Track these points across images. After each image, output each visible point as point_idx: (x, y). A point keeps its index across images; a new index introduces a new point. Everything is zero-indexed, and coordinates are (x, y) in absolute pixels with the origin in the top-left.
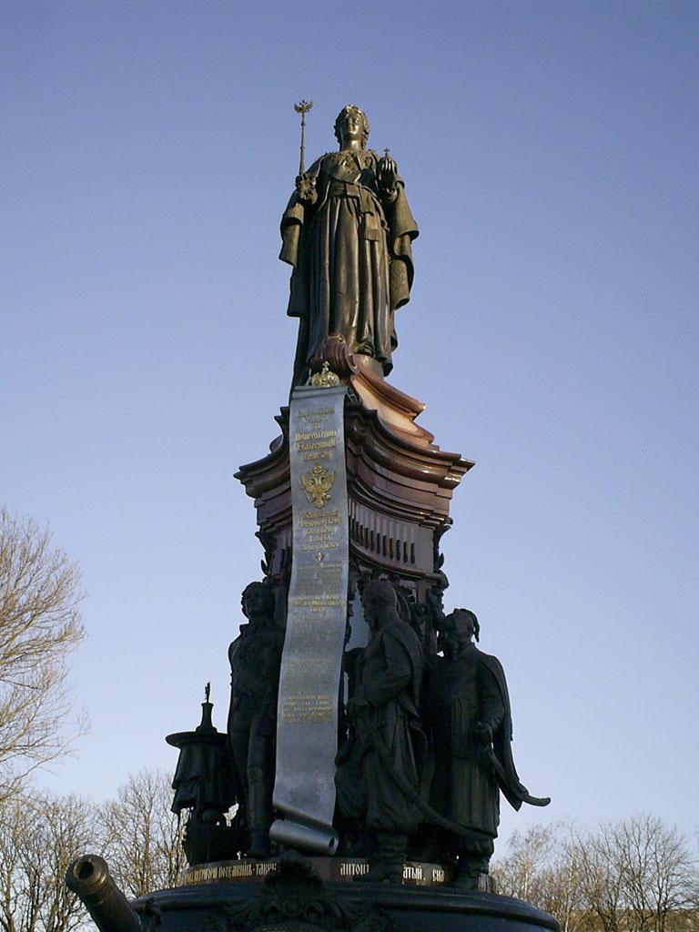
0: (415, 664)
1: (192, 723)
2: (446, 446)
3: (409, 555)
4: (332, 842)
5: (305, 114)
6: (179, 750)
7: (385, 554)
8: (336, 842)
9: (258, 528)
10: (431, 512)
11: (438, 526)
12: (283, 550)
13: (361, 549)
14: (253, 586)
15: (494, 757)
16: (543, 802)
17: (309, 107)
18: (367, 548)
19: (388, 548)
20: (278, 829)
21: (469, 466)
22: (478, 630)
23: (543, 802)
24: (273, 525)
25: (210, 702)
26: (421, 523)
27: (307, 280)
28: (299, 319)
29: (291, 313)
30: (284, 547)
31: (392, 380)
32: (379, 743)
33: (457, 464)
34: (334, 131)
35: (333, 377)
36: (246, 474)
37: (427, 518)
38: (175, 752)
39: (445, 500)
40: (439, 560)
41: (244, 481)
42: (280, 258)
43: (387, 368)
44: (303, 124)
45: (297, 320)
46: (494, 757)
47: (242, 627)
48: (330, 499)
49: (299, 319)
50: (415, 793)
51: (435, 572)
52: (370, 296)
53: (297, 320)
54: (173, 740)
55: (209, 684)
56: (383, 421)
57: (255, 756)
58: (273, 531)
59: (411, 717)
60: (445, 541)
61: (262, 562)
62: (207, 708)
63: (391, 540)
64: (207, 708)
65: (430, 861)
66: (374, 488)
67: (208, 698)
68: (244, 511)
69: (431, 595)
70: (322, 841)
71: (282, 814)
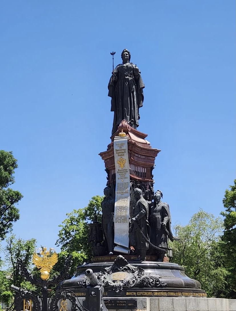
0: (147, 210)
4: (129, 252)
12: (112, 175)
13: (133, 176)
14: (105, 188)
17: (115, 53)
20: (116, 249)
21: (158, 152)
22: (162, 195)
28: (114, 112)
29: (112, 111)
31: (138, 129)
34: (122, 59)
42: (109, 95)
44: (113, 59)
49: (114, 112)
52: (133, 106)
58: (110, 169)
61: (107, 177)
63: (140, 172)
68: (101, 164)
71: (116, 245)
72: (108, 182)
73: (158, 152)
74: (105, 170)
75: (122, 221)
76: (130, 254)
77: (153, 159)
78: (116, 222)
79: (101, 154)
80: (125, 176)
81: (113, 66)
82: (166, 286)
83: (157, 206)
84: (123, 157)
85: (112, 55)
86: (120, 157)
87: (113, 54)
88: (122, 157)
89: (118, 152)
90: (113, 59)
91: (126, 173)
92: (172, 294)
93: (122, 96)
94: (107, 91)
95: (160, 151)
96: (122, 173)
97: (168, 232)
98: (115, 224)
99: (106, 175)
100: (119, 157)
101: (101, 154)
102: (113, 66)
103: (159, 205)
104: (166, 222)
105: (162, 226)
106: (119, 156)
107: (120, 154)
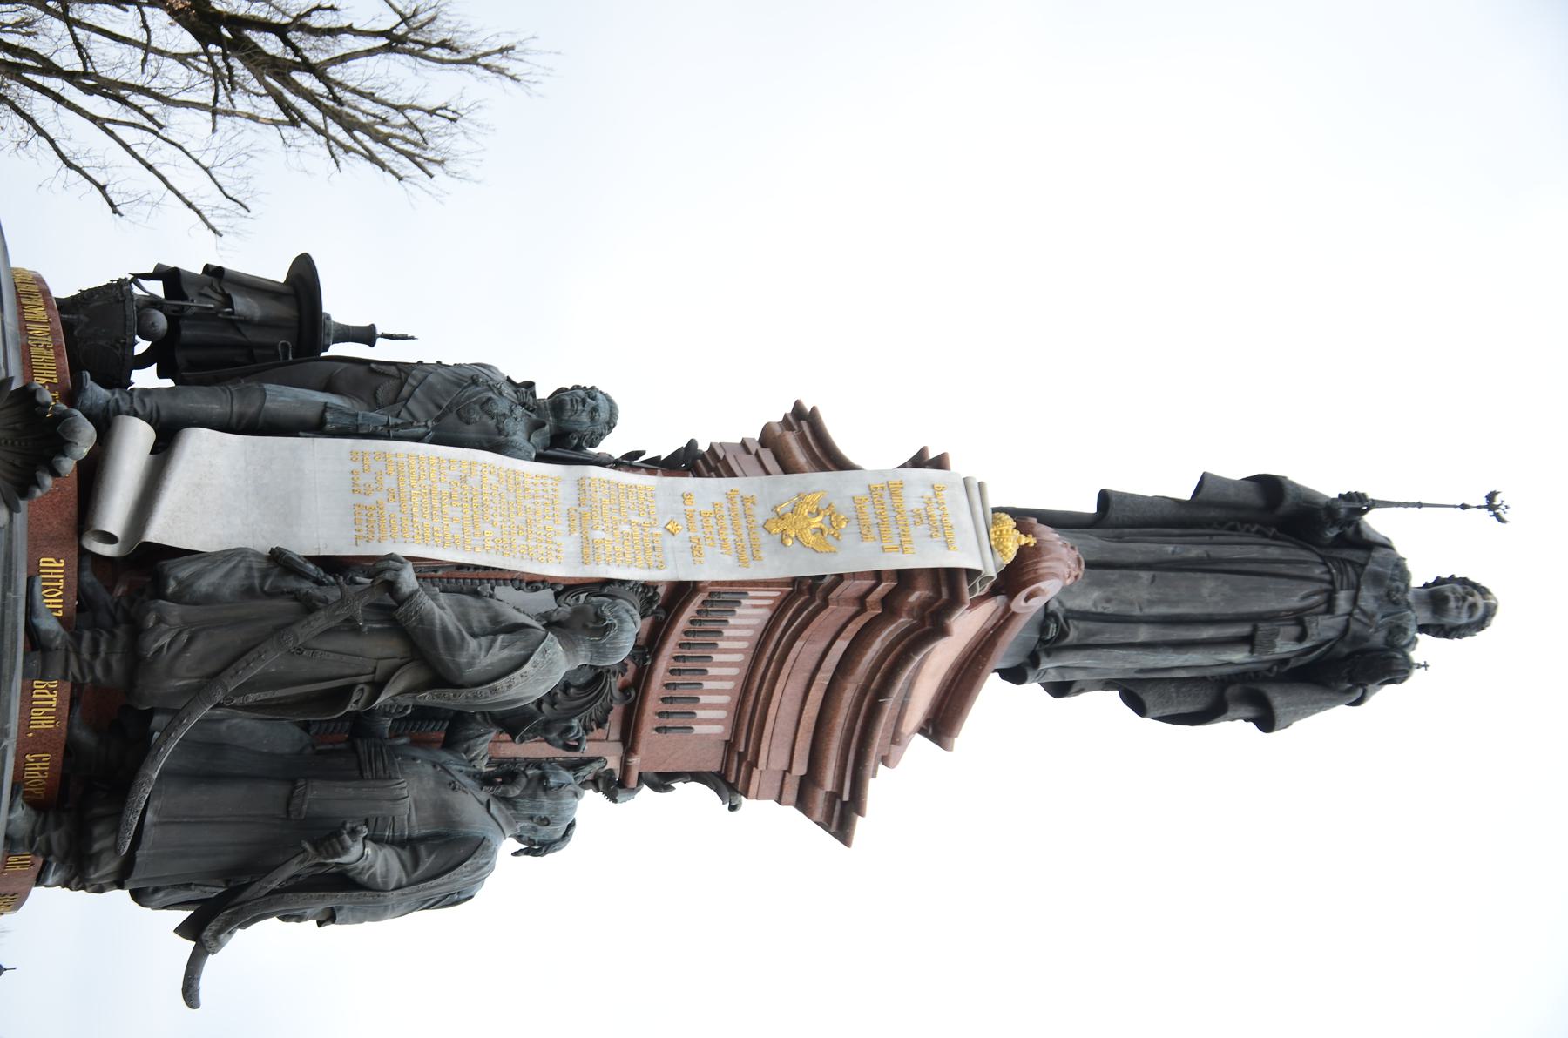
3: (670, 722)
4: (109, 538)
7: (672, 672)
8: (108, 550)
9: (703, 447)
10: (754, 764)
15: (293, 868)
16: (190, 993)
18: (692, 622)
19: (699, 640)
21: (843, 832)
23: (190, 993)
25: (379, 341)
26: (730, 745)
31: (993, 688)
32: (320, 621)
36: (803, 420)
37: (742, 756)
38: (278, 273)
39: (777, 791)
40: (662, 781)
41: (790, 418)
42: (1204, 479)
43: (1015, 675)
44: (1464, 507)
45: (1090, 507)
46: (293, 868)
47: (530, 385)
48: (785, 545)
50: (219, 697)
51: (640, 774)
53: (1090, 507)
55: (412, 338)
56: (930, 652)
57: (283, 398)
59: (378, 687)
60: (695, 797)
65: (71, 749)
66: (799, 644)
69: (596, 766)
70: (114, 515)
71: (164, 446)
73: (843, 832)
74: (692, 444)
75: (370, 501)
76: (83, 553)
77: (791, 791)
80: (705, 549)
81: (1420, 505)
83: (483, 796)
85: (1484, 502)
87: (1491, 502)
88: (855, 529)
90: (1464, 507)
91: (733, 551)
93: (1227, 567)
94: (1236, 467)
96: (727, 522)
97: (274, 886)
102: (1420, 505)
103: (493, 808)
104: (361, 864)
105: (329, 835)
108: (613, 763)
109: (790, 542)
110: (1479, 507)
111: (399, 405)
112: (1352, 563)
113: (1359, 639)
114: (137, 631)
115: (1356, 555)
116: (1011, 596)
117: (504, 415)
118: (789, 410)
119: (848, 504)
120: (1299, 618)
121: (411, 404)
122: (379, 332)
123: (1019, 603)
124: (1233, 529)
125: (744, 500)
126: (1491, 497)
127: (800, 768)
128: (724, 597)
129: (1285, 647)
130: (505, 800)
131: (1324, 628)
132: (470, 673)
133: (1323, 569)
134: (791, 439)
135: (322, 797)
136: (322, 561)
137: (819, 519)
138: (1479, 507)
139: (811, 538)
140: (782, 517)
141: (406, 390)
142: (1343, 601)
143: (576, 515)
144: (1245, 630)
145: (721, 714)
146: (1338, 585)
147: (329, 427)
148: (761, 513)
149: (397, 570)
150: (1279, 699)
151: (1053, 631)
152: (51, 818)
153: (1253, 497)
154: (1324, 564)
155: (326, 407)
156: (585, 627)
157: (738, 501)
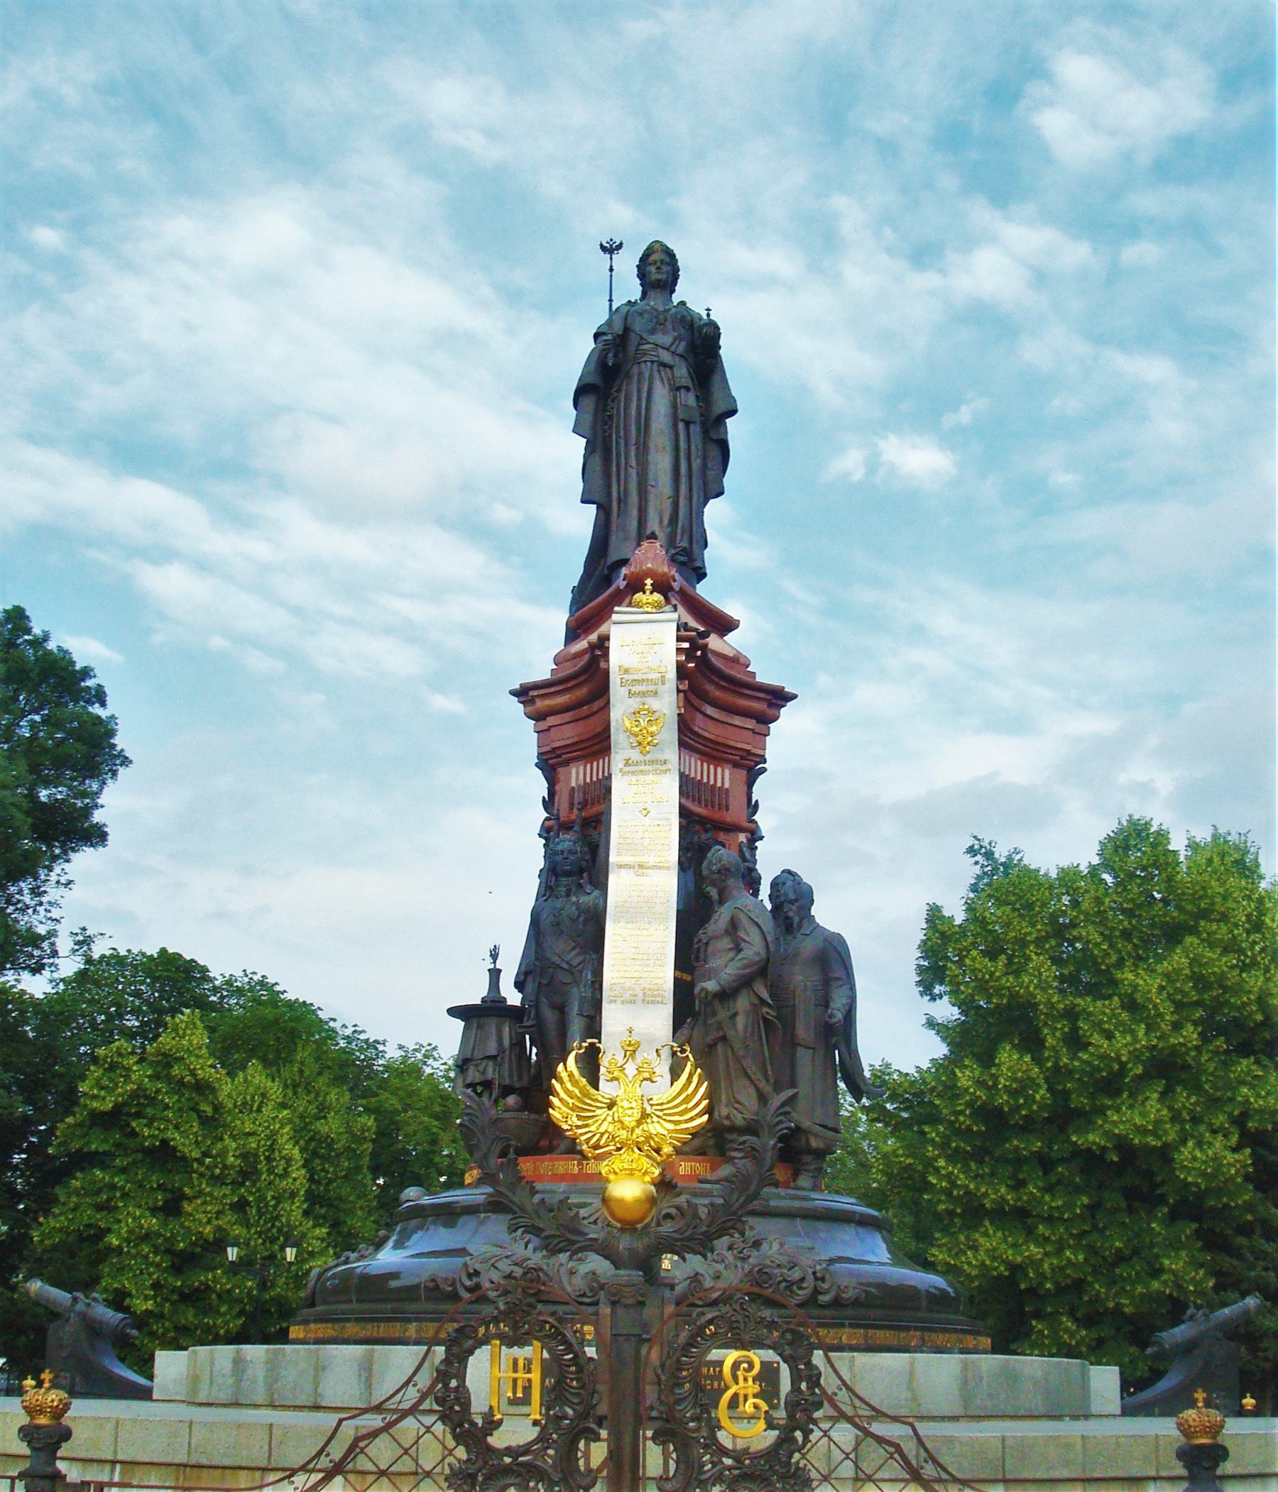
1: (475, 994)
2: (765, 673)
5: (614, 256)
6: (463, 1023)
11: (751, 766)
17: (620, 246)
24: (559, 756)
26: (735, 765)
27: (607, 460)
30: (573, 784)
32: (730, 1034)
33: (779, 698)
35: (657, 597)
38: (459, 1025)
41: (522, 699)
42: (574, 431)
44: (611, 270)
54: (455, 1012)
62: (495, 974)
64: (495, 974)
67: (495, 962)
72: (547, 819)
74: (536, 765)
75: (640, 995)
78: (611, 1002)
79: (524, 693)
81: (611, 300)
82: (856, 1303)
83: (799, 936)
84: (654, 704)
85: (608, 256)
86: (639, 699)
89: (631, 677)
90: (611, 270)
92: (881, 1336)
95: (794, 697)
98: (605, 1006)
99: (540, 786)
100: (634, 703)
101: (524, 693)
102: (611, 300)
106: (631, 694)
107: (634, 689)
108: (742, 838)
109: (655, 741)
110: (611, 259)
111: (574, 970)
112: (639, 345)
113: (686, 350)
114: (733, 1129)
115: (634, 340)
116: (671, 589)
117: (577, 908)
118: (516, 699)
119: (631, 701)
120: (676, 389)
121: (574, 963)
122: (492, 966)
123: (676, 585)
124: (610, 417)
125: (627, 764)
126: (603, 248)
127: (750, 724)
128: (688, 786)
129: (690, 399)
130: (800, 926)
131: (682, 372)
132: (763, 954)
133: (643, 365)
134: (540, 704)
135: (804, 1031)
136: (678, 1024)
137: (641, 720)
138: (611, 259)
139: (653, 729)
140: (640, 744)
141: (565, 966)
142: (666, 357)
143: (641, 871)
144: (681, 426)
145: (719, 770)
146: (656, 359)
147: (592, 1013)
148: (635, 755)
149: (707, 991)
150: (719, 407)
151: (682, 559)
152: (804, 1167)
153: (589, 402)
154: (639, 363)
155: (581, 1014)
156: (724, 881)
157: (627, 769)
